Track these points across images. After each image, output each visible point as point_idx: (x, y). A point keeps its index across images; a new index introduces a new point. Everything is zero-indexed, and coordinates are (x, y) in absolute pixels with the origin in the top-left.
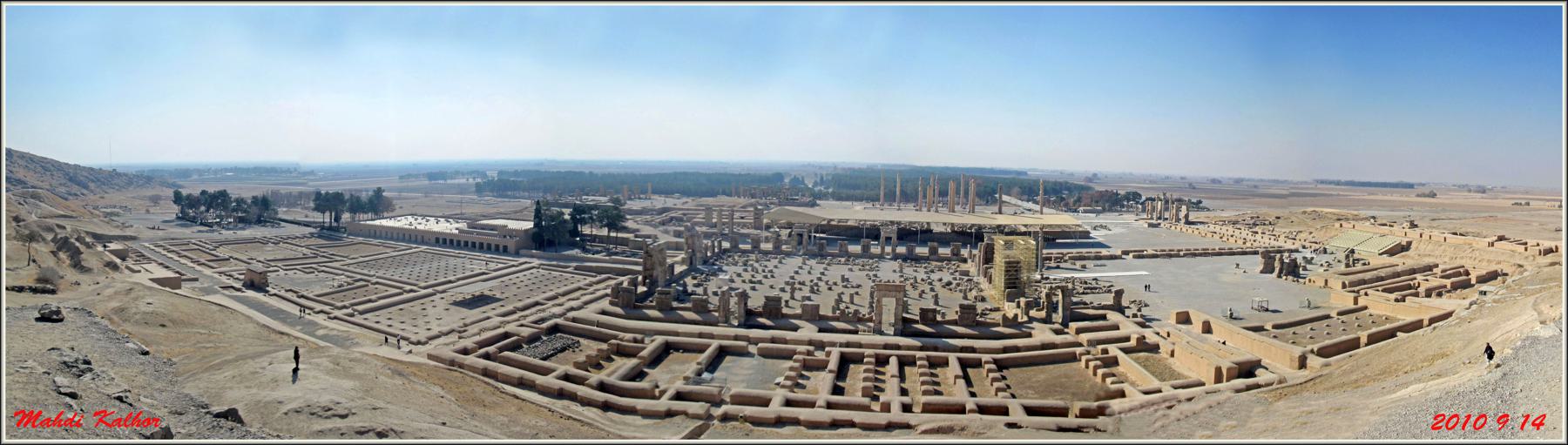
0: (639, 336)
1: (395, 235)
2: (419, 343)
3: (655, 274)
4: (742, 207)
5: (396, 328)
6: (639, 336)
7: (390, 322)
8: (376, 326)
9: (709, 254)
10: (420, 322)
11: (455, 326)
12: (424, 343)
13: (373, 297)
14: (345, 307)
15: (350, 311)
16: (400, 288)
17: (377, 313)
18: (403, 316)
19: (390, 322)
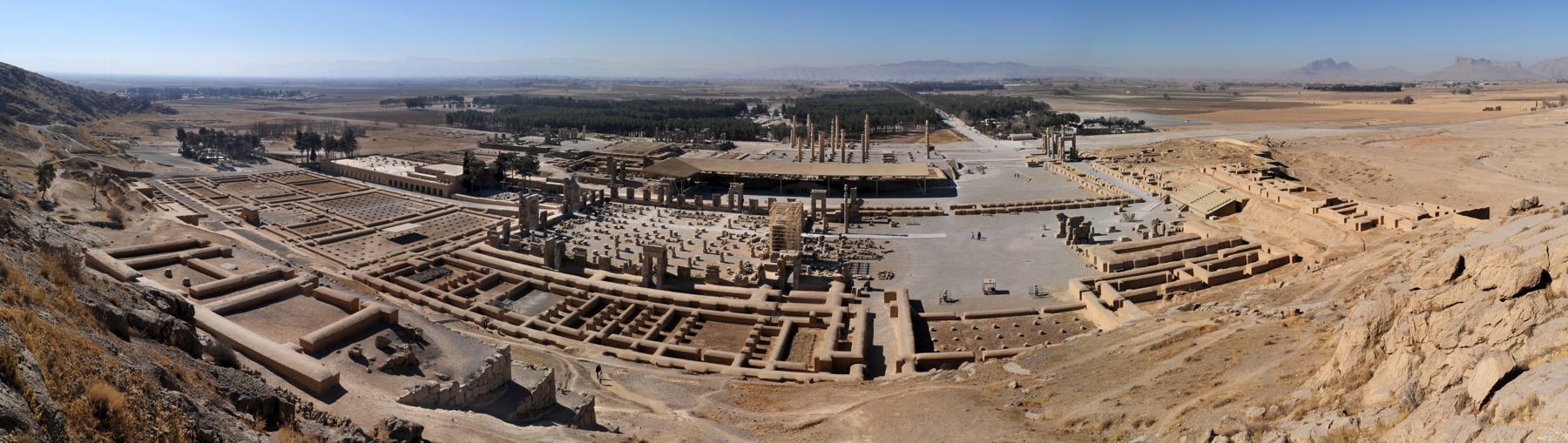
0: (485, 268)
1: (350, 173)
2: (352, 268)
3: (527, 220)
4: (650, 154)
5: (341, 257)
6: (485, 268)
7: (337, 252)
8: (328, 255)
9: (588, 203)
10: (358, 254)
11: (379, 258)
12: (357, 269)
13: (329, 232)
14: (307, 238)
15: (312, 241)
16: (351, 225)
17: (330, 245)
18: (347, 248)
19: (337, 252)
